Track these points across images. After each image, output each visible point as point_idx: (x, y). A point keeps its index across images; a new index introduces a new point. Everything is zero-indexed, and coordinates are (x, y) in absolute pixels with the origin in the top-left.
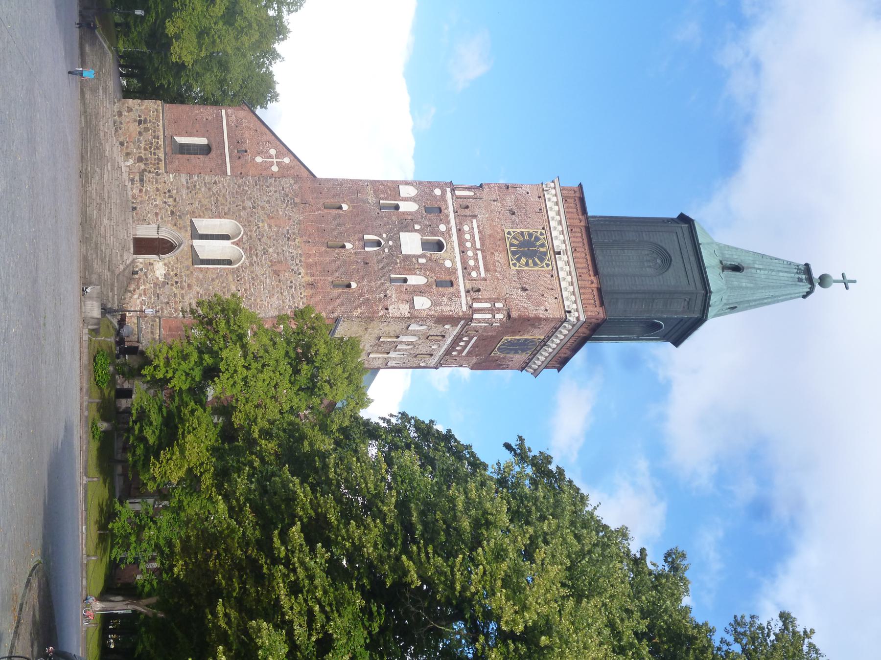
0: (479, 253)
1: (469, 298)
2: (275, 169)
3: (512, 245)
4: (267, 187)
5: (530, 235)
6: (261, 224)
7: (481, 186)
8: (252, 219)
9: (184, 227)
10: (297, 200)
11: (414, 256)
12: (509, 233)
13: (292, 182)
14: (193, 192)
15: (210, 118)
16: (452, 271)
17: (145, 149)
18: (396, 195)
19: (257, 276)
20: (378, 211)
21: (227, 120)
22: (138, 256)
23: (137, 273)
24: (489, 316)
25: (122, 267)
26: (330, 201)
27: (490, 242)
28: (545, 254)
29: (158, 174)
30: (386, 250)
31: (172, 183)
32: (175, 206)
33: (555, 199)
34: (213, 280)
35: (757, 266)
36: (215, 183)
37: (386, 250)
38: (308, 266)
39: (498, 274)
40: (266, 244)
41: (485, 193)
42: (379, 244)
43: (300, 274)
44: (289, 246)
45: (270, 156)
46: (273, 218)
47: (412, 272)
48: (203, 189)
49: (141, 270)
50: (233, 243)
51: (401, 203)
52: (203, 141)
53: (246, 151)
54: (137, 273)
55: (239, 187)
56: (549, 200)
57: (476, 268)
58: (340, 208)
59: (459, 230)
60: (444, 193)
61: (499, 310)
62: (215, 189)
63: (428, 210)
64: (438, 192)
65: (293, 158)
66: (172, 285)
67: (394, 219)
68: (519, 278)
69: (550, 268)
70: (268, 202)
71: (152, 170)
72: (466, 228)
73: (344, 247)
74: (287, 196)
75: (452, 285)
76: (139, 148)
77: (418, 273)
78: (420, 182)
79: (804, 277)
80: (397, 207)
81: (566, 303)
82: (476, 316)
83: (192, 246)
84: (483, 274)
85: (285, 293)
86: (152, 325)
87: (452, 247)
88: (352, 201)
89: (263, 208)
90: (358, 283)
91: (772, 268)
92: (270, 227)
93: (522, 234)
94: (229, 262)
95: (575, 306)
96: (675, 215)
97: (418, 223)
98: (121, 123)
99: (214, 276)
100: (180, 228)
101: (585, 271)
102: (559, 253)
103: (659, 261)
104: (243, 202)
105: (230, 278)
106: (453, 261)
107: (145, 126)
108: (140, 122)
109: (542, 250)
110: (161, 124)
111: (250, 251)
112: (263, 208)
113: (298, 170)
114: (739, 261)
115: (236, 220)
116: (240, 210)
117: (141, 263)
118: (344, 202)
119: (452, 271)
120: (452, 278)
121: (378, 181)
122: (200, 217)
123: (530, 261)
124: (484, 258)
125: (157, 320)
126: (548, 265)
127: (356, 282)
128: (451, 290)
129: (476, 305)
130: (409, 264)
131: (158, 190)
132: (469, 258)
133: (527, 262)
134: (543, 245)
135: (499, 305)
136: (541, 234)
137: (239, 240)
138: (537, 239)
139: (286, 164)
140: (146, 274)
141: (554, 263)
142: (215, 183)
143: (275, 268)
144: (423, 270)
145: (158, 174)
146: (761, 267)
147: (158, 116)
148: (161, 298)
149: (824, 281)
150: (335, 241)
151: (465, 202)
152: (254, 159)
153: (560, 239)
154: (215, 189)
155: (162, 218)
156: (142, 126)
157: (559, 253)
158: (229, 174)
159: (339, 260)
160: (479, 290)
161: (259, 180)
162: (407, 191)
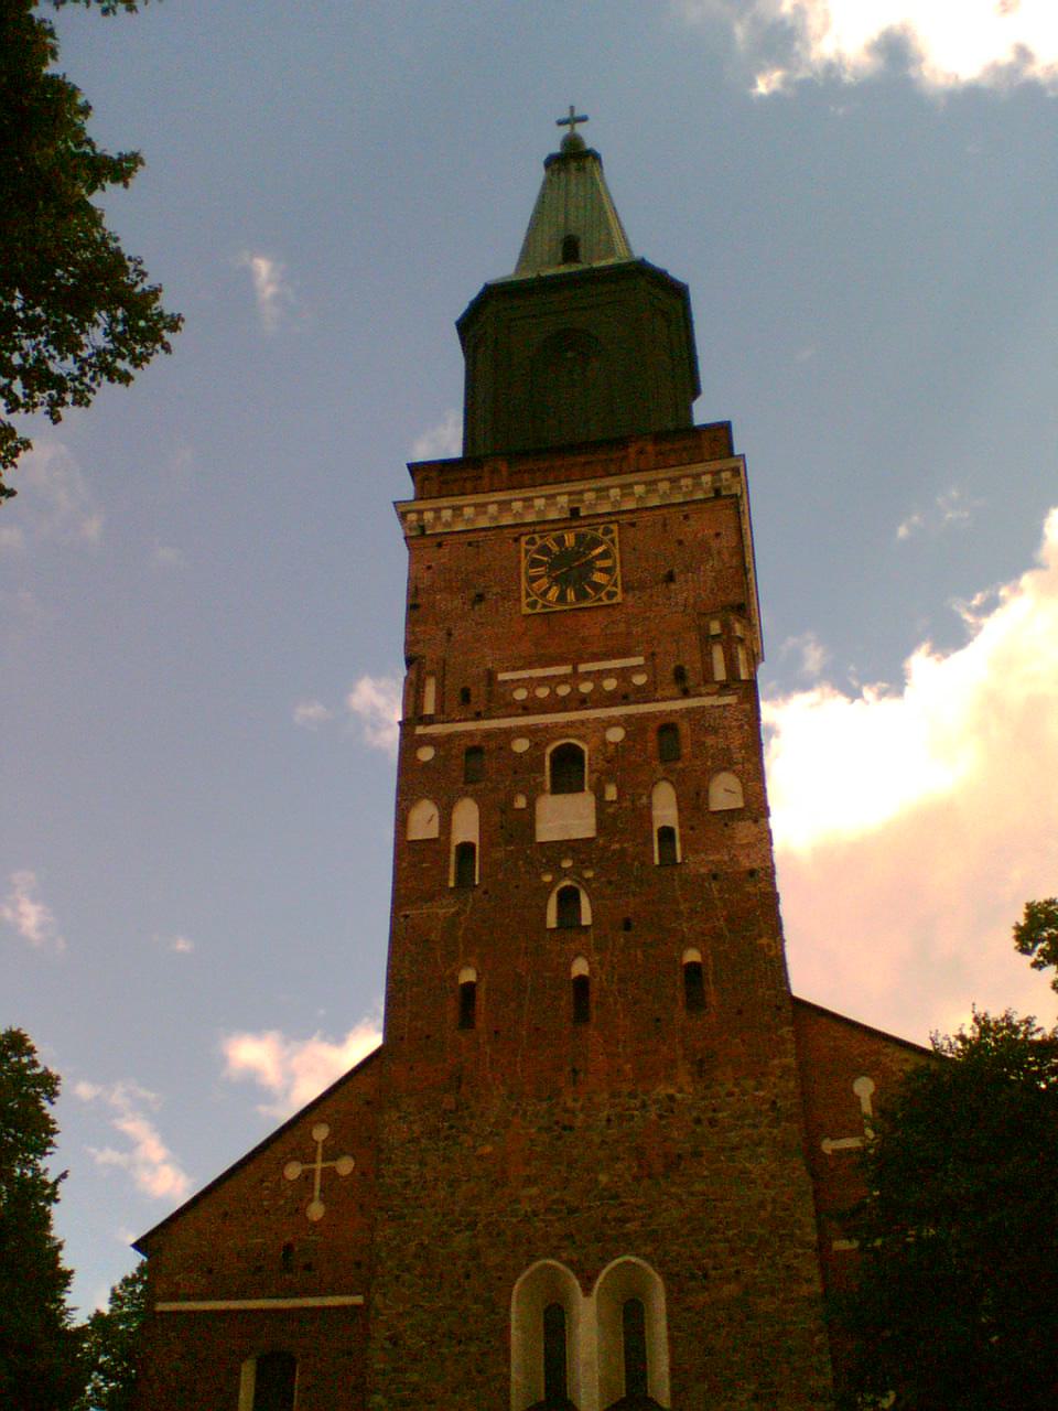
0: (583, 668)
1: (703, 690)
2: (345, 1166)
3: (562, 598)
4: (408, 1183)
10: (449, 1101)
12: (533, 605)
13: (394, 1115)
21: (188, 1298)
27: (554, 639)
30: (589, 874)
35: (561, 220)
37: (589, 874)
39: (637, 630)
42: (568, 899)
45: (307, 1177)
46: (504, 1172)
47: (645, 815)
48: (415, 1377)
50: (587, 1291)
53: (288, 1248)
55: (408, 1269)
56: (447, 524)
57: (624, 674)
58: (470, 987)
59: (526, 709)
61: (727, 627)
64: (426, 754)
65: (314, 1116)
68: (642, 586)
69: (614, 527)
72: (521, 695)
73: (582, 984)
77: (644, 800)
78: (400, 791)
80: (466, 850)
81: (700, 496)
82: (743, 676)
84: (639, 660)
85: (734, 1137)
97: (511, 800)
102: (575, 512)
109: (570, 540)
114: (554, 243)
118: (454, 977)
119: (634, 726)
120: (653, 725)
121: (395, 890)
123: (599, 564)
124: (596, 658)
126: (607, 531)
129: (720, 674)
132: (598, 688)
133: (601, 570)
134: (560, 541)
135: (715, 628)
136: (532, 542)
138: (545, 550)
150: (566, 1000)
152: (315, 1225)
153: (545, 503)
157: (575, 512)
158: (359, 1300)
162: (425, 821)
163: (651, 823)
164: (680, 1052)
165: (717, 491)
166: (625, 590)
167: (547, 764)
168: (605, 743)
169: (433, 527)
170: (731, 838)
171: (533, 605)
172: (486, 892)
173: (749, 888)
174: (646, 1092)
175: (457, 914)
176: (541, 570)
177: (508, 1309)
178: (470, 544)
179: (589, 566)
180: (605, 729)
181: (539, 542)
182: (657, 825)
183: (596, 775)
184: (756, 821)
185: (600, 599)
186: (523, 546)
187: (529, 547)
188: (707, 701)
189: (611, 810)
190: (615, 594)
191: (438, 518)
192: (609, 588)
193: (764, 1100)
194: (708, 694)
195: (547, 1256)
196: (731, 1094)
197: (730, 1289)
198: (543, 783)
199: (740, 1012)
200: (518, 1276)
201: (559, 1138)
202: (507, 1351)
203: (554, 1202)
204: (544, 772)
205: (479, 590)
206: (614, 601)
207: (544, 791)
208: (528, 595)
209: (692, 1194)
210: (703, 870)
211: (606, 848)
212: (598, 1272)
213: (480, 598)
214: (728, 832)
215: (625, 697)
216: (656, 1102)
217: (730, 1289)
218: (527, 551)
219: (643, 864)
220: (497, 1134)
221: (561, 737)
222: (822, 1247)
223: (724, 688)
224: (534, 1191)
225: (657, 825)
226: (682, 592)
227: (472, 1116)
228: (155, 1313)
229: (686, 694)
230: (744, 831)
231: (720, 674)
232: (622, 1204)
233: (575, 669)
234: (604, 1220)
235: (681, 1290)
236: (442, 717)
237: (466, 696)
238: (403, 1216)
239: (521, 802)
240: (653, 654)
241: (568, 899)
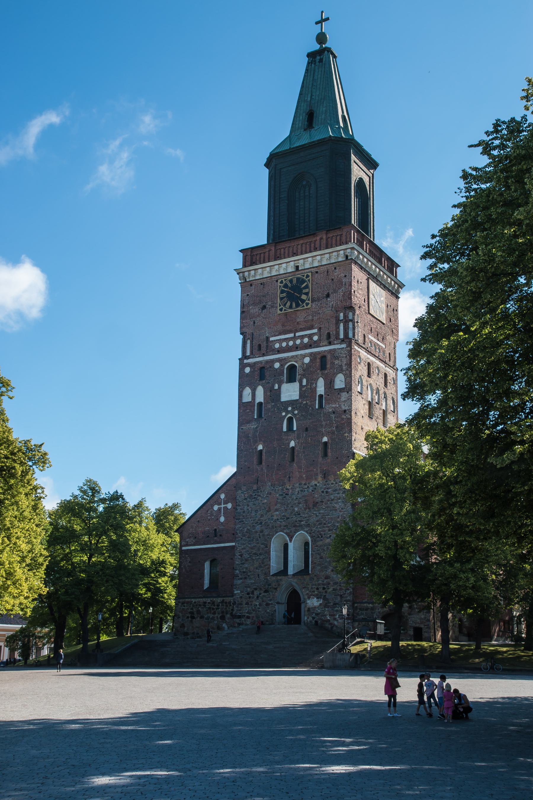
0: (298, 334)
1: (335, 342)
2: (229, 506)
3: (291, 307)
5: (282, 292)
6: (275, 518)
7: (241, 334)
8: (270, 526)
9: (277, 581)
10: (255, 487)
11: (300, 389)
12: (281, 310)
13: (240, 492)
14: (249, 574)
15: (189, 560)
17: (214, 613)
18: (251, 404)
19: (318, 521)
20: (263, 420)
22: (302, 621)
23: (316, 622)
25: (311, 634)
26: (255, 460)
27: (289, 325)
28: (298, 279)
29: (234, 603)
30: (296, 412)
31: (242, 592)
32: (261, 589)
33: (252, 273)
34: (321, 558)
35: (309, 99)
36: (241, 555)
37: (296, 412)
38: (309, 478)
39: (315, 318)
40: (292, 513)
41: (248, 331)
42: (290, 420)
43: (316, 485)
44: (293, 494)
45: (219, 509)
46: (269, 508)
47: (314, 390)
48: (246, 566)
49: (313, 618)
50: (291, 541)
52: (207, 565)
53: (215, 530)
54: (316, 622)
55: (244, 536)
57: (310, 336)
59: (279, 351)
60: (248, 365)
61: (345, 316)
62: (246, 556)
63: (262, 377)
64: (247, 370)
66: (326, 592)
67: (270, 407)
68: (319, 299)
69: (310, 274)
70: (256, 511)
71: (231, 608)
72: (277, 346)
74: (251, 496)
76: (213, 618)
77: (314, 385)
79: (318, 58)
80: (260, 404)
81: (340, 259)
83: (294, 575)
84: (315, 331)
86: (360, 609)
87: (292, 357)
88: (256, 443)
89: (262, 516)
90: (323, 436)
91: (310, 86)
92: (277, 510)
93: (281, 299)
94: (306, 544)
95: (342, 252)
96: (267, 171)
97: (273, 386)
98: (193, 633)
99: (318, 557)
100: (279, 585)
101: (313, 245)
103: (304, 183)
104: (256, 532)
105: (320, 543)
106: (304, 356)
107: (195, 613)
108: (193, 618)
109: (295, 281)
110: (193, 600)
111: (297, 527)
112: (262, 516)
113: (230, 487)
114: (304, 114)
115: (271, 539)
116: (263, 535)
117: (308, 618)
118: (256, 448)
120: (319, 357)
122: (269, 568)
123: (304, 291)
125: (356, 605)
126: (308, 276)
127: (322, 438)
128: (329, 357)
129: (342, 336)
130: (307, 393)
131: (247, 604)
136: (282, 282)
137: (288, 536)
139: (226, 497)
140: (317, 614)
141: (306, 271)
142: (241, 555)
143: (311, 506)
144: (312, 382)
145: (234, 603)
146: (310, 95)
147: (188, 603)
148: (337, 601)
149: (321, 38)
150: (288, 455)
151: (257, 347)
152: (222, 523)
154: (246, 556)
155: (271, 600)
156: (196, 616)
157: (297, 267)
158: (233, 544)
159: (304, 452)
160: (329, 334)
161: (239, 519)
162: (247, 398)
163: (316, 393)
165: (347, 257)
167: (285, 372)
168: (303, 363)
169: (249, 278)
170: (340, 398)
171: (281, 310)
172: (265, 420)
173: (344, 417)
174: (309, 484)
175: (257, 427)
177: (270, 546)
178: (261, 284)
179: (301, 293)
180: (304, 358)
181: (284, 282)
182: (318, 394)
183: (300, 376)
184: (348, 392)
185: (303, 306)
187: (281, 285)
190: (309, 303)
191: (249, 274)
192: (307, 301)
194: (337, 344)
195: (280, 531)
196: (332, 484)
198: (283, 380)
199: (337, 458)
201: (285, 497)
202: (270, 558)
204: (284, 376)
206: (308, 307)
207: (283, 383)
208: (280, 306)
209: (320, 513)
210: (330, 410)
211: (302, 403)
212: (293, 536)
213: (264, 307)
214: (339, 396)
215: (311, 346)
216: (312, 486)
218: (280, 286)
221: (289, 362)
223: (343, 341)
224: (278, 513)
225: (318, 394)
226: (332, 301)
227: (261, 492)
228: (182, 550)
229: (330, 344)
230: (344, 395)
231: (342, 336)
233: (295, 335)
234: (296, 521)
236: (252, 356)
238: (243, 521)
240: (320, 328)
241: (290, 420)
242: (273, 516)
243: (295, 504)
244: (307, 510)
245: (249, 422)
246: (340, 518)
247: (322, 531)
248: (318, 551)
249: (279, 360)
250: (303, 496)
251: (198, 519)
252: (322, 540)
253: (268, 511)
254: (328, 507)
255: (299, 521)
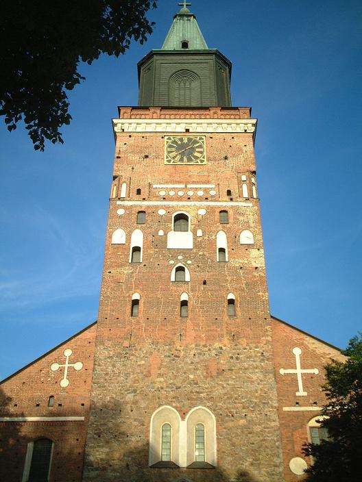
0: (189, 186)
2: (78, 366)
3: (181, 160)
4: (107, 374)
5: (170, 146)
6: (158, 385)
10: (126, 343)
12: (169, 161)
13: (102, 347)
16: (211, 210)
19: (225, 394)
24: (254, 188)
30: (189, 262)
34: (233, 445)
35: (181, 35)
37: (189, 262)
43: (221, 348)
44: (185, 356)
45: (61, 370)
46: (149, 372)
47: (214, 243)
50: (183, 418)
51: (133, 245)
57: (206, 190)
60: (123, 207)
65: (64, 346)
70: (127, 375)
72: (163, 193)
75: (226, 212)
77: (214, 237)
80: (136, 249)
84: (213, 186)
85: (246, 365)
87: (183, 206)
88: (129, 289)
89: (136, 381)
90: (228, 291)
92: (160, 375)
102: (187, 131)
105: (231, 424)
106: (200, 208)
109: (185, 141)
114: (178, 42)
116: (138, 408)
119: (211, 210)
124: (194, 183)
128: (231, 212)
129: (246, 195)
132: (195, 195)
134: (181, 140)
137: (180, 411)
138: (175, 142)
139: (74, 353)
143: (214, 373)
144: (210, 232)
152: (64, 389)
164: (225, 330)
166: (208, 160)
168: (197, 215)
170: (248, 254)
173: (255, 274)
176: (173, 149)
178: (143, 137)
186: (166, 140)
188: (240, 204)
189: (199, 240)
193: (258, 352)
195: (166, 404)
197: (243, 422)
200: (154, 411)
201: (173, 360)
203: (170, 384)
205: (147, 154)
208: (167, 157)
211: (197, 253)
212: (187, 412)
213: (147, 157)
214: (247, 252)
215: (207, 199)
216: (215, 349)
217: (243, 422)
218: (167, 142)
219: (212, 261)
220: (147, 357)
222: (279, 409)
224: (162, 379)
225: (218, 247)
227: (136, 350)
229: (231, 199)
232: (199, 386)
233: (186, 186)
234: (192, 392)
235: (222, 420)
237: (139, 192)
238: (105, 386)
239: (161, 233)
242: (154, 383)
243: (190, 370)
244: (209, 379)
245: (121, 266)
246: (259, 392)
247: (232, 408)
248: (228, 434)
249: (166, 208)
250: (202, 361)
251: (24, 381)
252: (233, 421)
253: (146, 376)
254: (240, 377)
255: (196, 392)
